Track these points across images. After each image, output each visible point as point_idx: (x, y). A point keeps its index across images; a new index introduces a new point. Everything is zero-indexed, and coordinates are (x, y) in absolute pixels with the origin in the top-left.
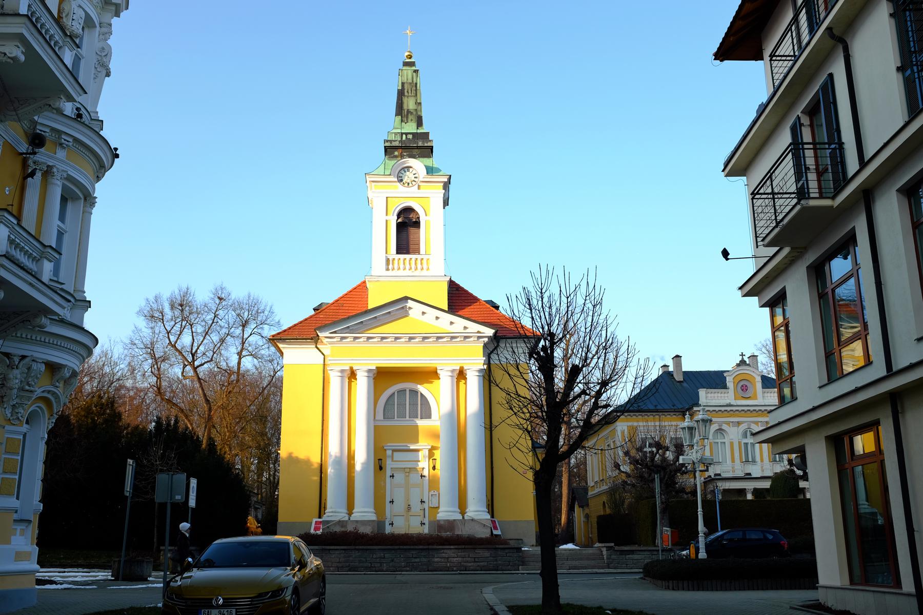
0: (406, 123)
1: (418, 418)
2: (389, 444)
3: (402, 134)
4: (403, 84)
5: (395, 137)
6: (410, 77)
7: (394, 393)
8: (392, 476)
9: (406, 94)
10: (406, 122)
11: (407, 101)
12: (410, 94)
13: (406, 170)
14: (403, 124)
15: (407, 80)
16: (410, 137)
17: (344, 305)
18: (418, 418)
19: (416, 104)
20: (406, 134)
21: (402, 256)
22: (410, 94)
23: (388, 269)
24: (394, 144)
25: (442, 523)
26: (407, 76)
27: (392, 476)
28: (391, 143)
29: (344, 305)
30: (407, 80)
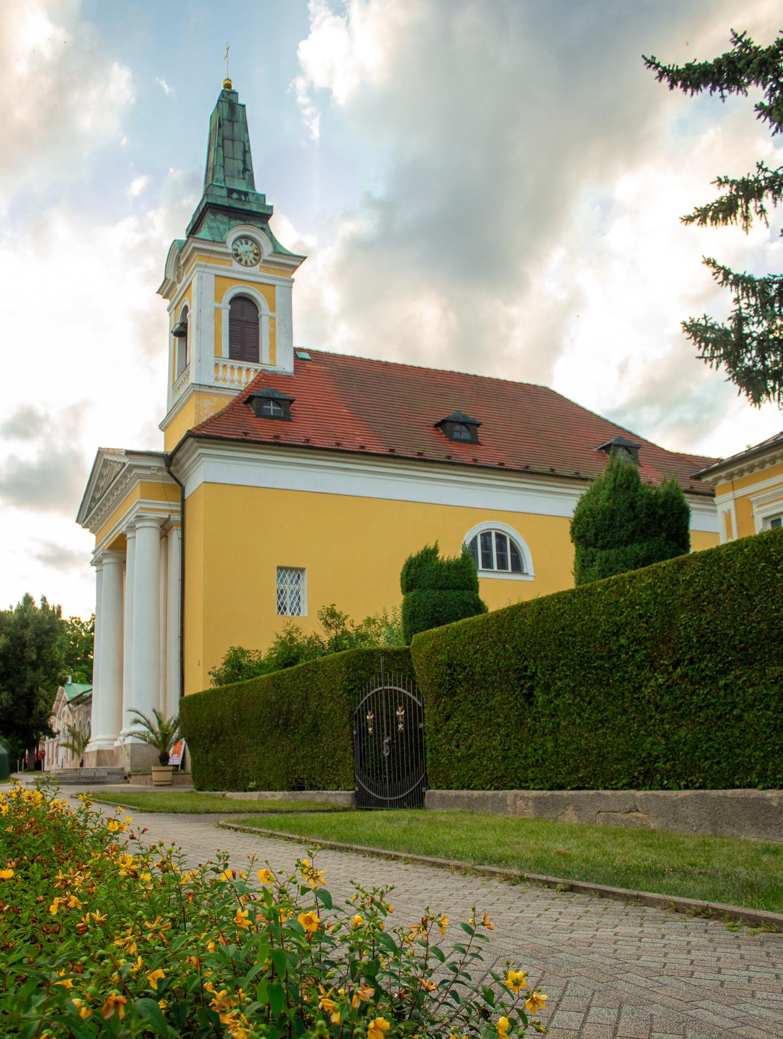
13: (243, 241)
21: (237, 363)
23: (217, 379)
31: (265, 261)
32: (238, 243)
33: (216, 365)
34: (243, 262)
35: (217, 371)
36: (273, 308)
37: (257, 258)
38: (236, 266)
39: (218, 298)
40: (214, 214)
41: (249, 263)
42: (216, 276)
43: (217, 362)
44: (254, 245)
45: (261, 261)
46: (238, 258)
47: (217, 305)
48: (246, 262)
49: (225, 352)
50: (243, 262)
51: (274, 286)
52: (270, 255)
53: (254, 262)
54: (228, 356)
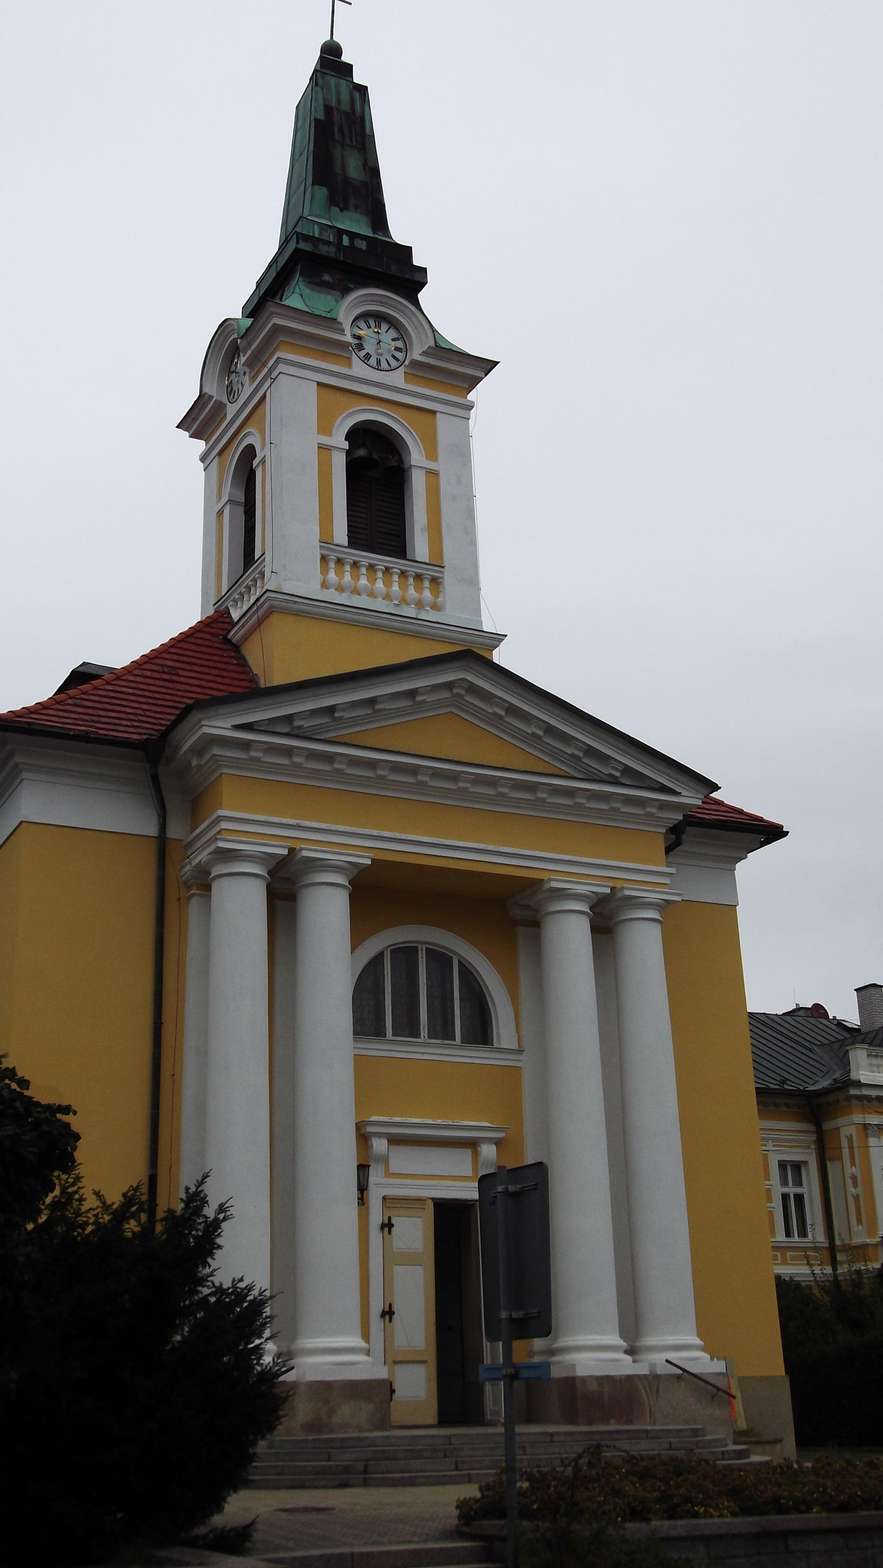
0: (342, 210)
1: (418, 1036)
2: (374, 1118)
3: (341, 232)
4: (328, 109)
5: (320, 233)
6: (345, 97)
7: (383, 952)
8: (387, 1226)
9: (337, 137)
10: (341, 205)
11: (342, 156)
12: (347, 141)
14: (333, 208)
15: (339, 101)
16: (362, 245)
17: (182, 673)
18: (418, 1036)
19: (364, 169)
20: (352, 236)
21: (366, 557)
22: (347, 141)
23: (324, 585)
24: (323, 249)
25: (593, 1387)
26: (338, 93)
27: (387, 1226)
28: (315, 246)
29: (182, 673)
30: (339, 101)
31: (414, 364)
32: (362, 324)
33: (323, 558)
34: (373, 361)
35: (324, 570)
36: (432, 453)
37: (400, 356)
38: (359, 369)
39: (324, 427)
40: (315, 281)
41: (384, 365)
42: (319, 384)
43: (325, 552)
44: (393, 334)
45: (407, 363)
46: (362, 354)
47: (326, 440)
48: (379, 362)
49: (341, 532)
50: (373, 361)
51: (434, 413)
52: (424, 353)
53: (394, 363)
54: (347, 544)
